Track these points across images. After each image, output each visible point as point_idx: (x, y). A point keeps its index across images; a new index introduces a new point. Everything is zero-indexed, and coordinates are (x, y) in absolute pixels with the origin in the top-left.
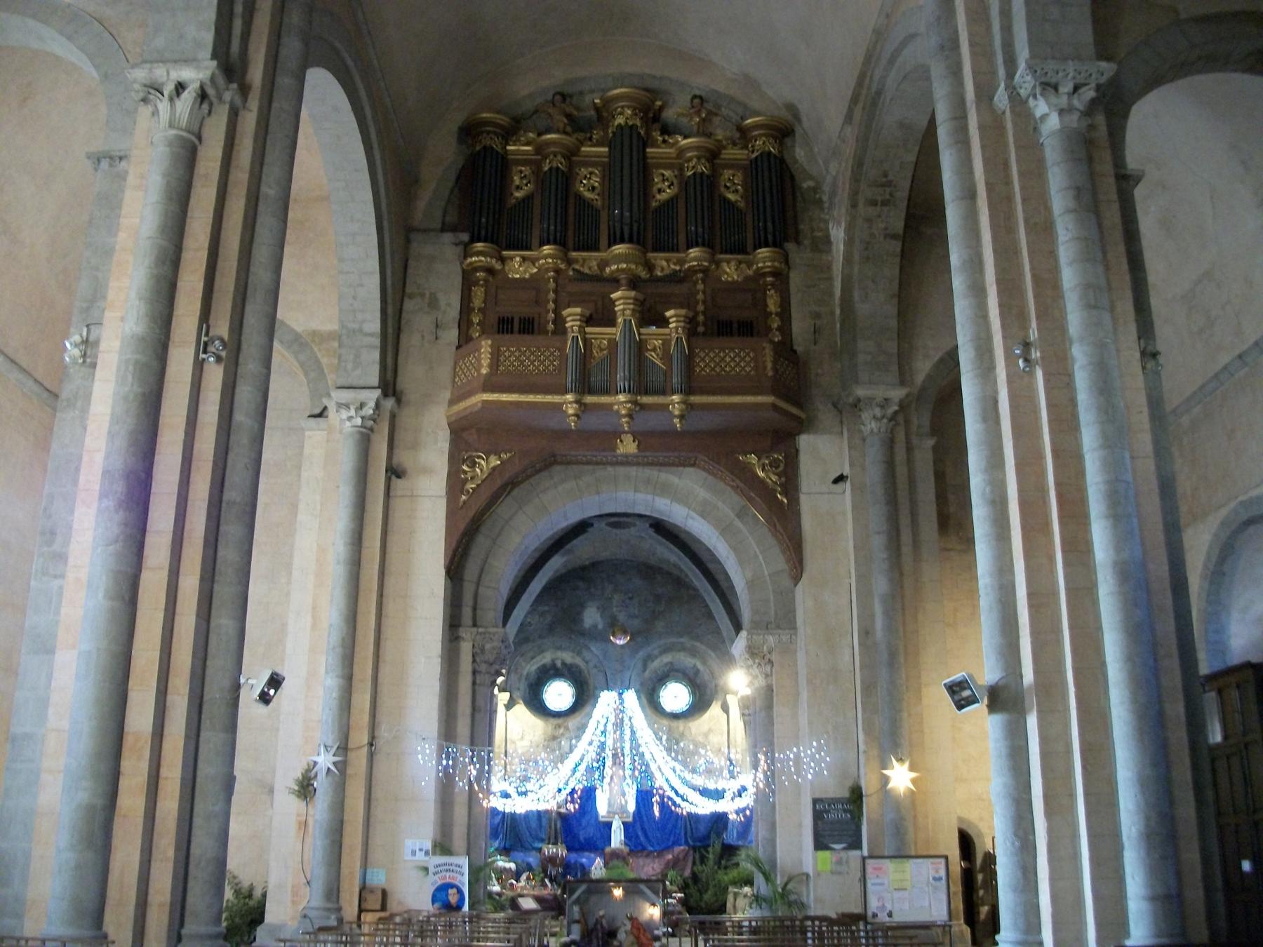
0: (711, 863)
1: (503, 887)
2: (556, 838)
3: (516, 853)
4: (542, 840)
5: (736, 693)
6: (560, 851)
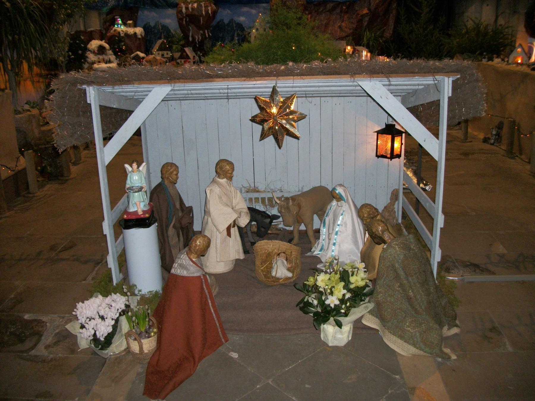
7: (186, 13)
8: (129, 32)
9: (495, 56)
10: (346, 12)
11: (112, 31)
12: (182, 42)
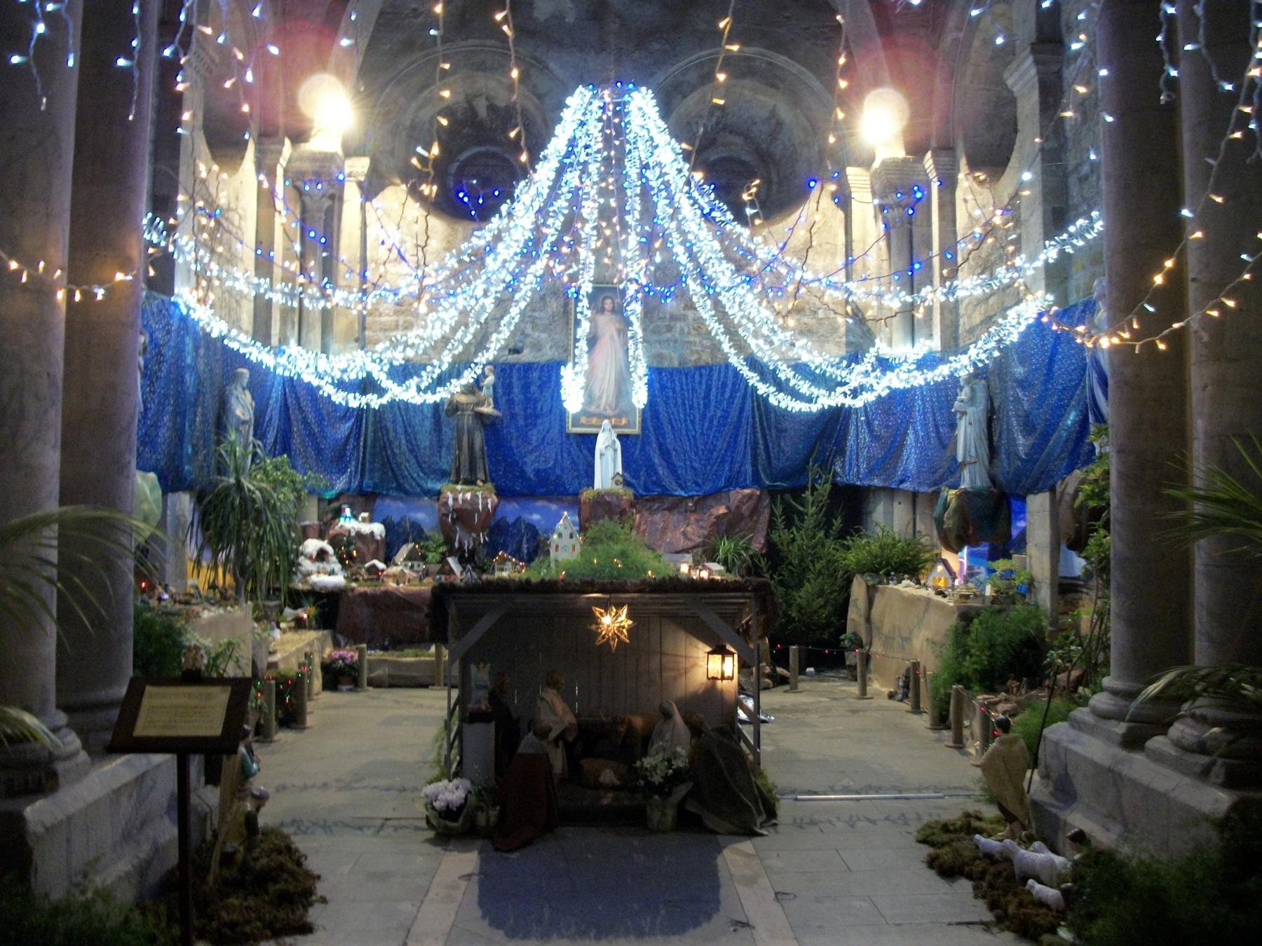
0: (809, 522)
1: (352, 578)
2: (472, 469)
3: (387, 501)
4: (444, 475)
5: (866, 163)
6: (482, 496)
8: (363, 531)
9: (906, 576)
10: (692, 512)
11: (337, 528)
12: (443, 549)
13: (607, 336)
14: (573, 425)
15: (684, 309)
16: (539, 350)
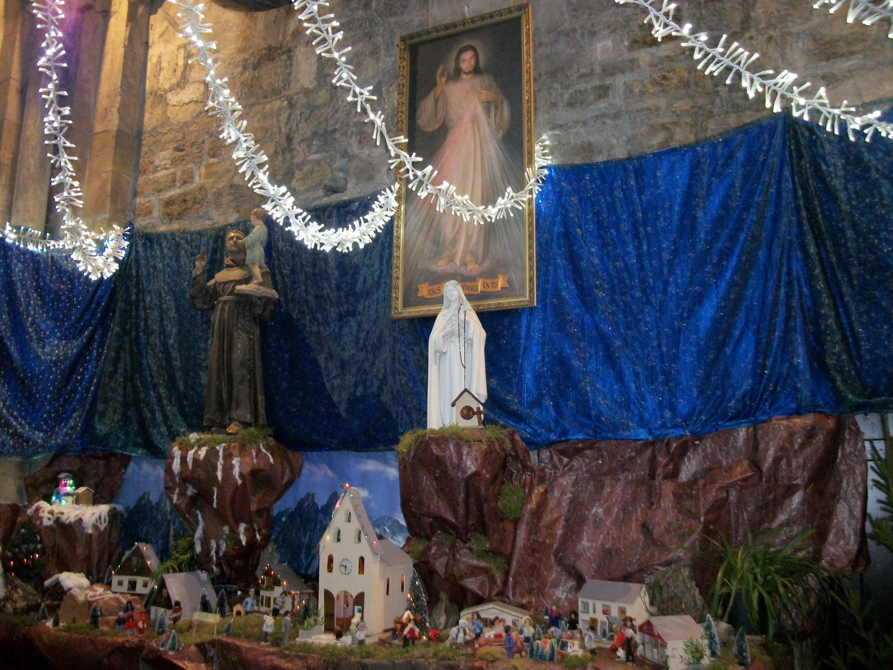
7: (181, 473)
13: (467, 118)
14: (405, 305)
15: (631, 48)
16: (371, 178)
